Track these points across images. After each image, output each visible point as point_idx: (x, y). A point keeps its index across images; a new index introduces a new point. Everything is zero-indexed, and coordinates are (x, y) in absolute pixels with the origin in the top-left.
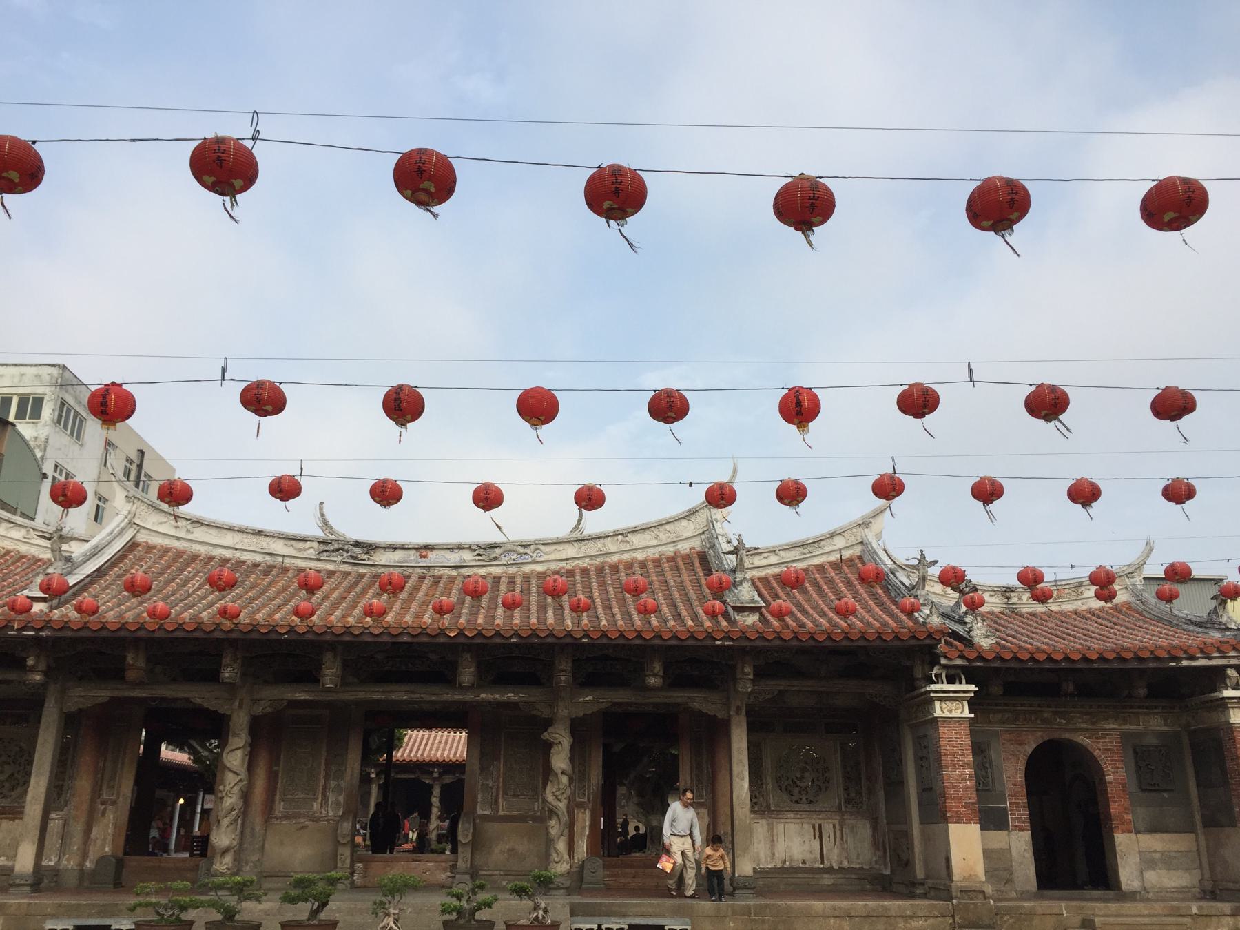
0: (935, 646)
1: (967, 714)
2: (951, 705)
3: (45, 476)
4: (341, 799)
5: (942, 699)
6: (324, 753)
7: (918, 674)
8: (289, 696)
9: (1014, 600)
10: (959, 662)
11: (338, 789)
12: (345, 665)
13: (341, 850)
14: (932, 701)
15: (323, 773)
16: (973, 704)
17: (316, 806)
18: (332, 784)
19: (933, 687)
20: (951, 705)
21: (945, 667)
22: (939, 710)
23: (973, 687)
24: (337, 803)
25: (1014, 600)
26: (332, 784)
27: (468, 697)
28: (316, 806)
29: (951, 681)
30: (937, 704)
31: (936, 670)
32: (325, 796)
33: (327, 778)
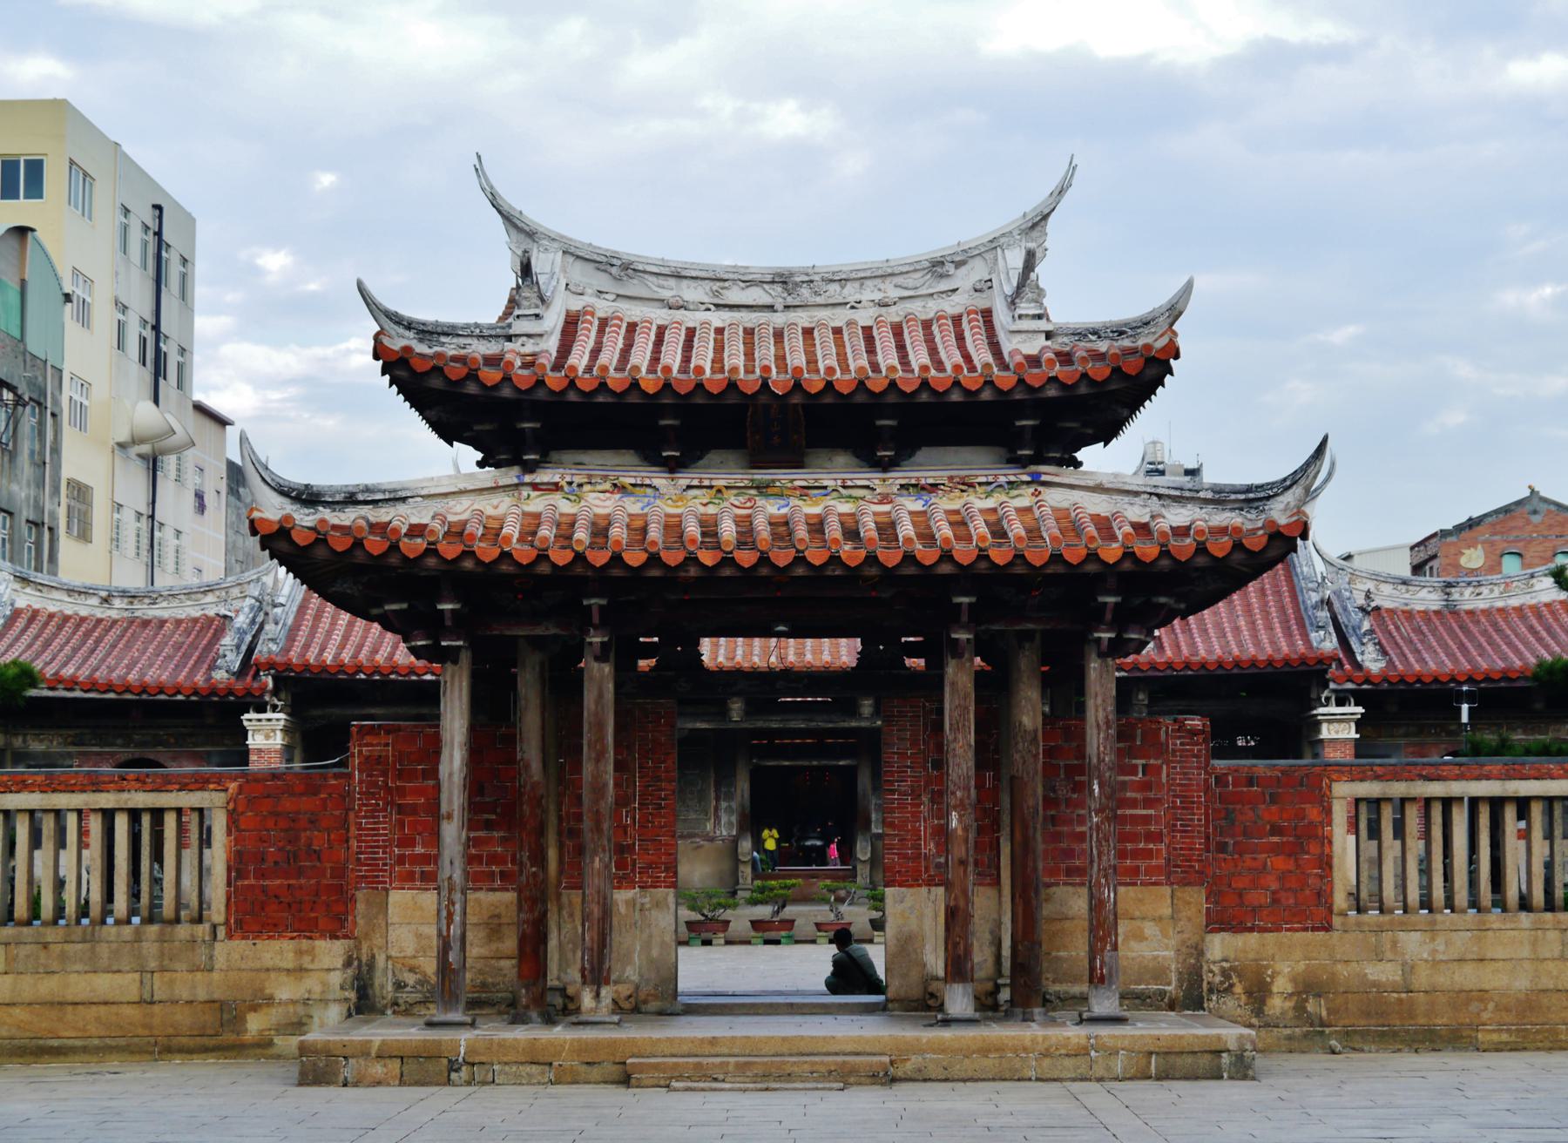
0: (1325, 671)
1: (1354, 735)
2: (1338, 726)
3: (68, 298)
4: (734, 819)
5: (1329, 721)
6: (712, 775)
7: (1314, 695)
8: (690, 726)
9: (1456, 596)
10: (1350, 686)
11: (729, 810)
12: (748, 703)
13: (741, 868)
14: (1319, 723)
15: (713, 795)
16: (1360, 725)
17: (709, 826)
18: (724, 805)
19: (1321, 710)
20: (1338, 726)
21: (1334, 691)
22: (1326, 732)
23: (1360, 710)
24: (730, 823)
25: (1456, 596)
26: (724, 805)
27: (863, 724)
28: (709, 826)
29: (1340, 703)
30: (1324, 726)
31: (1326, 693)
32: (717, 818)
33: (718, 799)
